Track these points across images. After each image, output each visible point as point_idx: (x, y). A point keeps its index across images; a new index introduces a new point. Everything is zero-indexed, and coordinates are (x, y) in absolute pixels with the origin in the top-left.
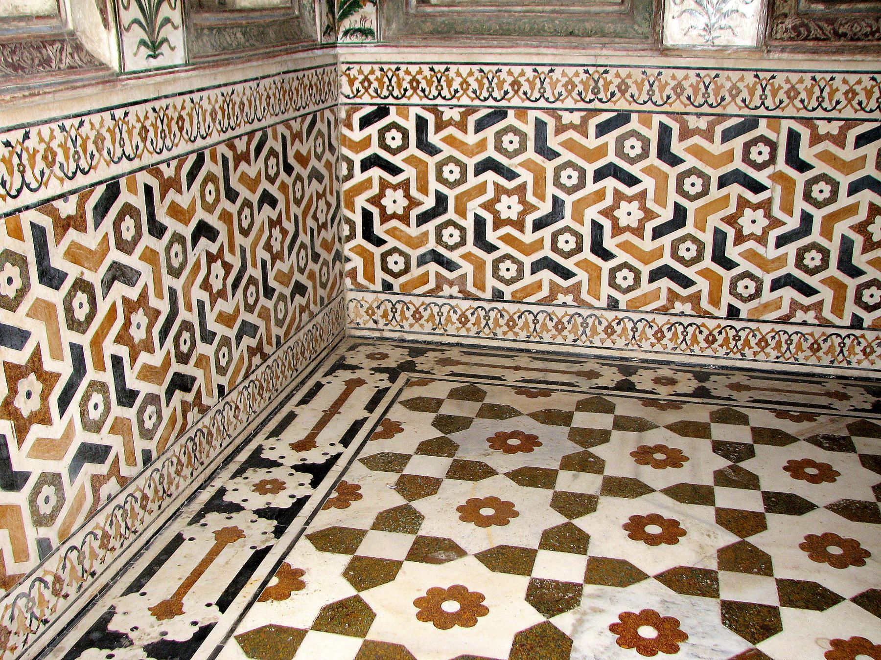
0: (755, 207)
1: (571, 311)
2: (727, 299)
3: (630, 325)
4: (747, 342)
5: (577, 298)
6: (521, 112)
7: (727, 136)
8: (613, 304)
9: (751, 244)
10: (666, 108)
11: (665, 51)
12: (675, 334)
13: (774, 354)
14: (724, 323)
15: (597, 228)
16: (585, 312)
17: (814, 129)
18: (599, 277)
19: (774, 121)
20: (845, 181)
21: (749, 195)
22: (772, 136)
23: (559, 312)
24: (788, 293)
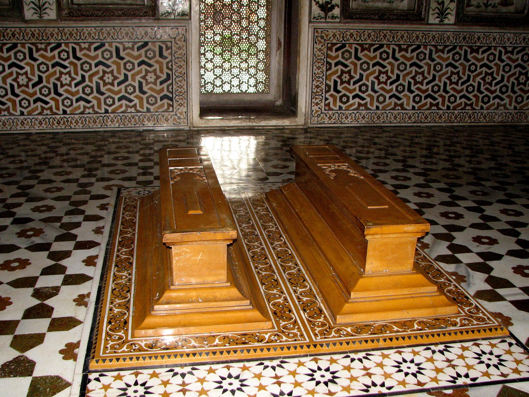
0: (65, 74)
1: (7, 117)
2: (61, 107)
3: (29, 121)
4: (71, 123)
5: (9, 112)
7: (52, 50)
8: (22, 114)
9: (66, 87)
10: (30, 41)
11: (26, 22)
12: (46, 122)
13: (81, 125)
14: (62, 116)
15: (12, 86)
16: (13, 117)
17: (80, 46)
19: (67, 44)
20: (93, 63)
21: (63, 70)
22: (67, 49)
24: (82, 103)
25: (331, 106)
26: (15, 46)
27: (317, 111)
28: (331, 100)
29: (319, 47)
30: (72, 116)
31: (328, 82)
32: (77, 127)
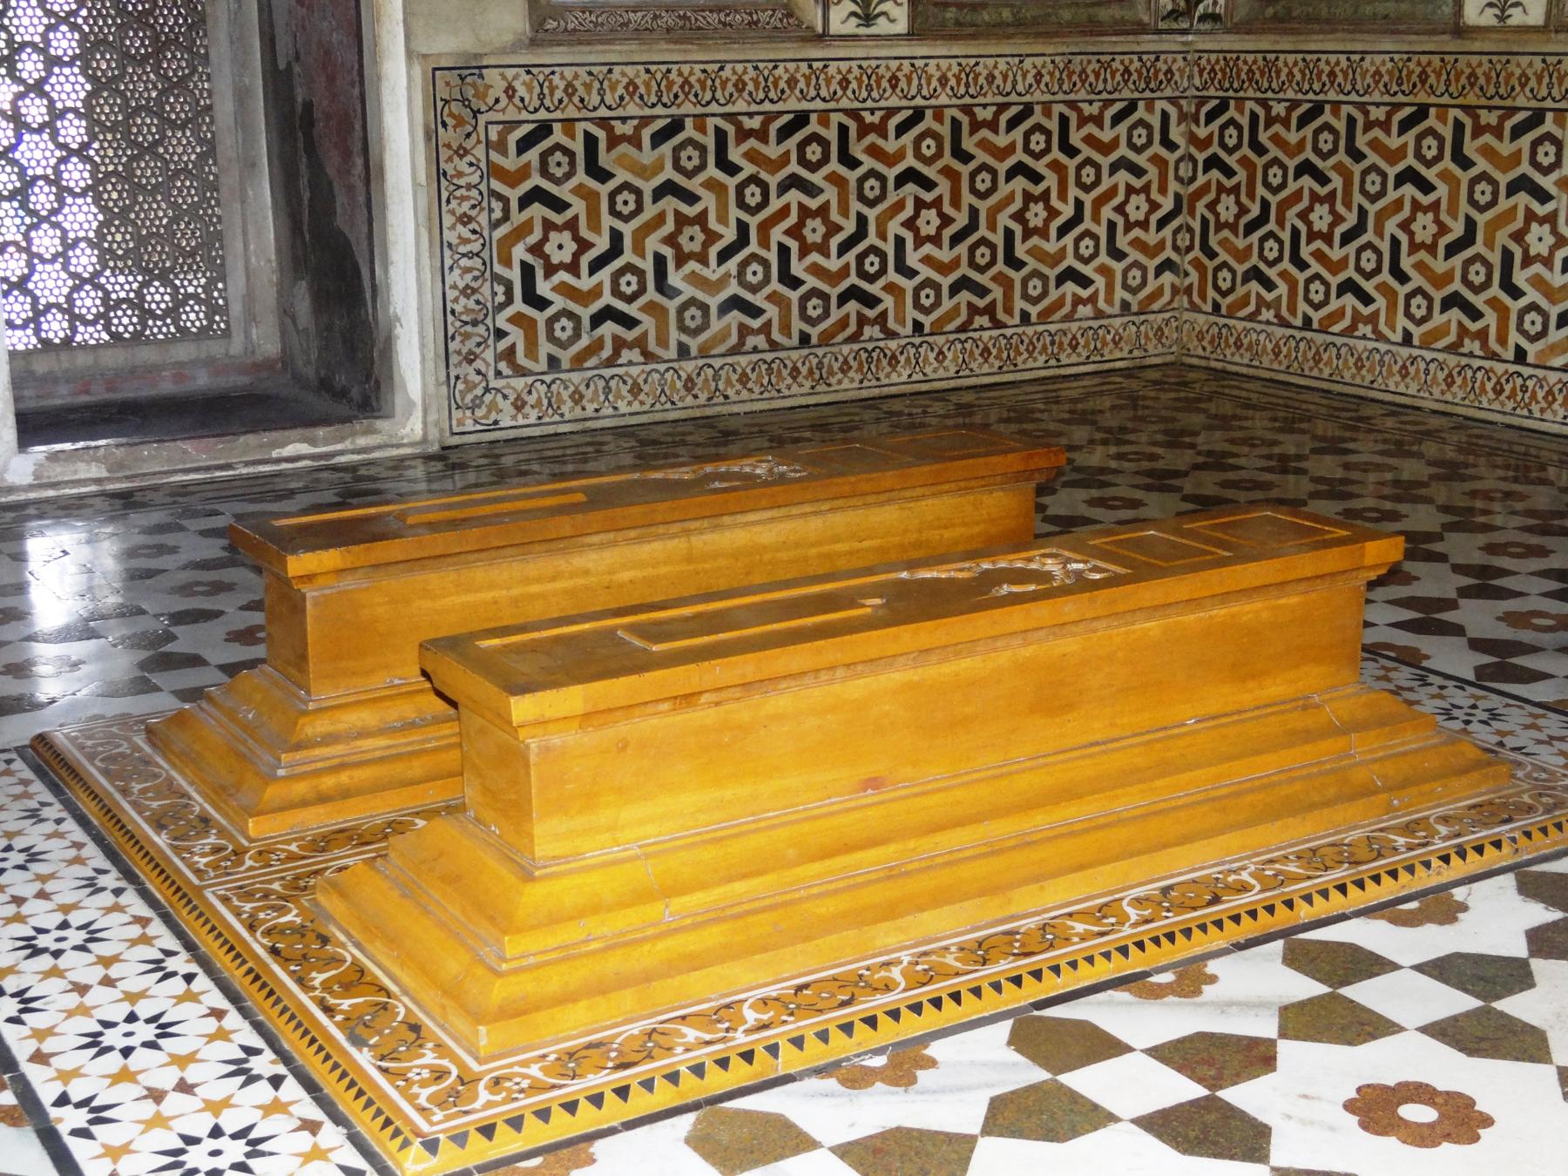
2: (1514, 337)
4: (1534, 396)
6: (1336, 105)
8: (1407, 339)
14: (1513, 368)
16: (1383, 347)
18: (1395, 304)
21: (1536, 206)
23: (1360, 345)
26: (1422, 112)
30: (1540, 373)
32: (1548, 415)
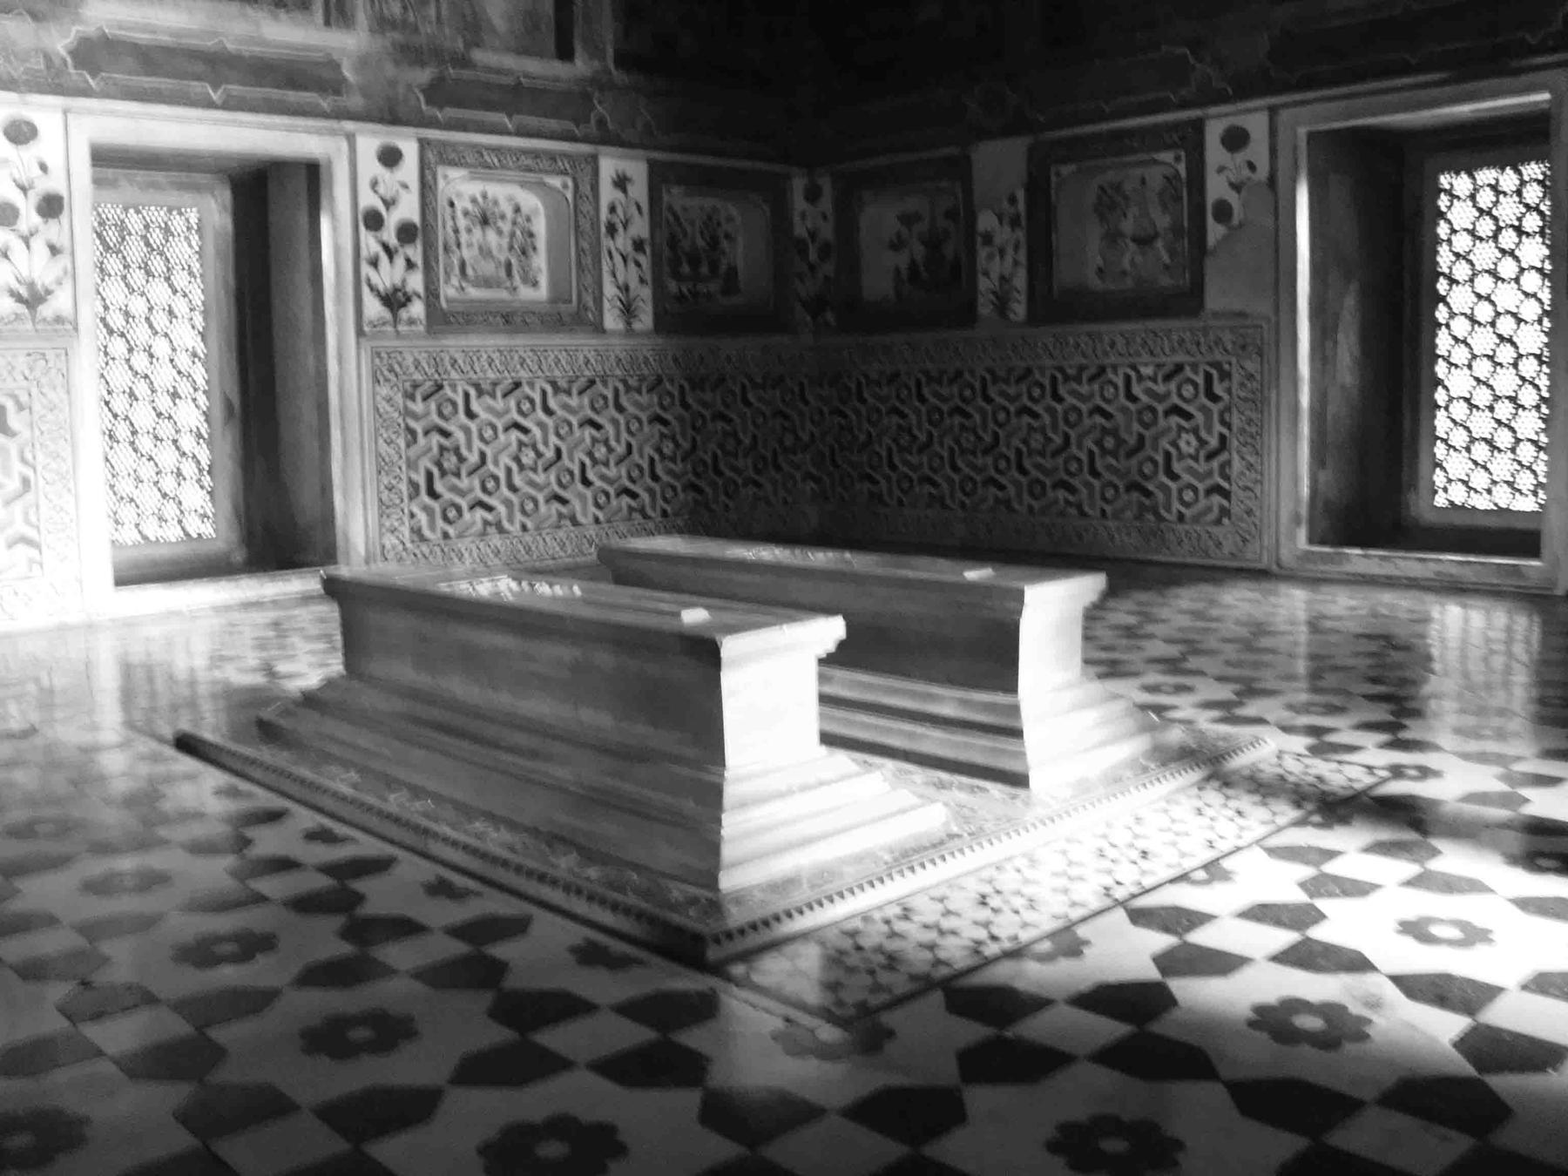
25: (427, 533)
27: (394, 547)
28: (422, 518)
29: (384, 390)
31: (414, 476)
